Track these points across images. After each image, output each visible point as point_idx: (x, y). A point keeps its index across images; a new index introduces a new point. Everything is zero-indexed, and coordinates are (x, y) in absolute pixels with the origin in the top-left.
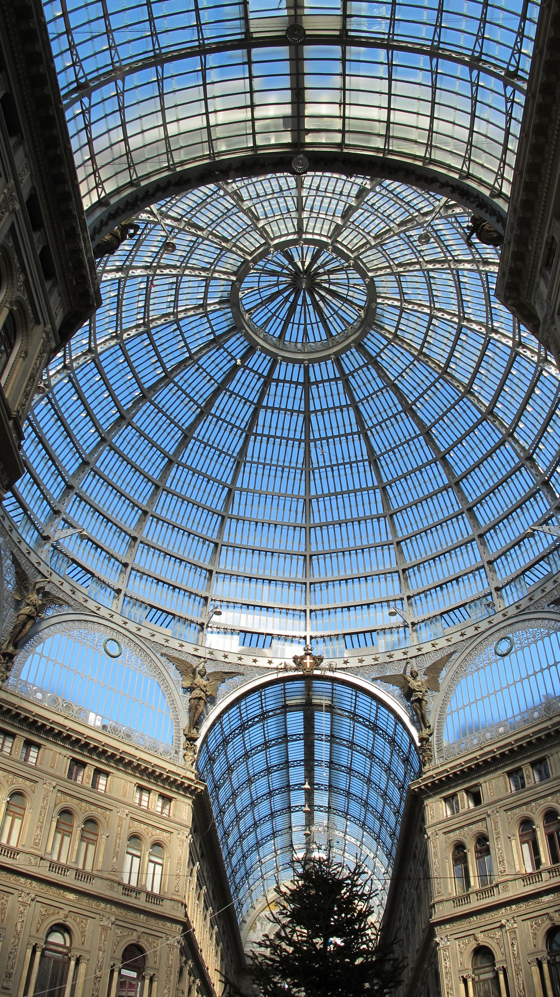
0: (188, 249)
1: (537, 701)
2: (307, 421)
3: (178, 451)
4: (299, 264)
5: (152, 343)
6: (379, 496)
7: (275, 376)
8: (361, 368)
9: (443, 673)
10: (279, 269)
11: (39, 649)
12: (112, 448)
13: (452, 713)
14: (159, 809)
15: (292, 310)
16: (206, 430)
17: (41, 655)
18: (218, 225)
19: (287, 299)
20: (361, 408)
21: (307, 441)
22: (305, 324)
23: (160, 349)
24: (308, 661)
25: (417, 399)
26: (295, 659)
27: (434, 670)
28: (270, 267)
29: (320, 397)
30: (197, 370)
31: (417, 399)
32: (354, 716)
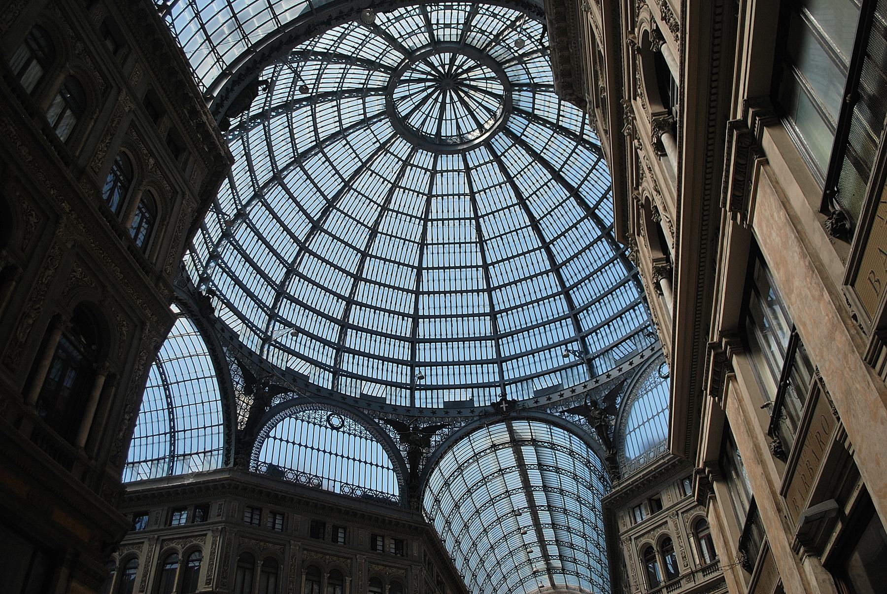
0: (340, 76)
2: (473, 201)
3: (368, 246)
4: (440, 68)
5: (328, 159)
6: (544, 253)
7: (439, 168)
8: (510, 148)
9: (619, 400)
10: (424, 76)
11: (272, 434)
12: (311, 253)
13: (630, 432)
14: (393, 551)
15: (443, 109)
16: (388, 224)
17: (275, 438)
18: (361, 50)
19: (436, 100)
20: (517, 182)
21: (477, 218)
22: (457, 119)
23: (335, 164)
24: (504, 405)
25: (563, 166)
26: (493, 404)
27: (611, 398)
28: (416, 76)
29: (480, 180)
30: (371, 175)
31: (563, 166)
32: (553, 446)
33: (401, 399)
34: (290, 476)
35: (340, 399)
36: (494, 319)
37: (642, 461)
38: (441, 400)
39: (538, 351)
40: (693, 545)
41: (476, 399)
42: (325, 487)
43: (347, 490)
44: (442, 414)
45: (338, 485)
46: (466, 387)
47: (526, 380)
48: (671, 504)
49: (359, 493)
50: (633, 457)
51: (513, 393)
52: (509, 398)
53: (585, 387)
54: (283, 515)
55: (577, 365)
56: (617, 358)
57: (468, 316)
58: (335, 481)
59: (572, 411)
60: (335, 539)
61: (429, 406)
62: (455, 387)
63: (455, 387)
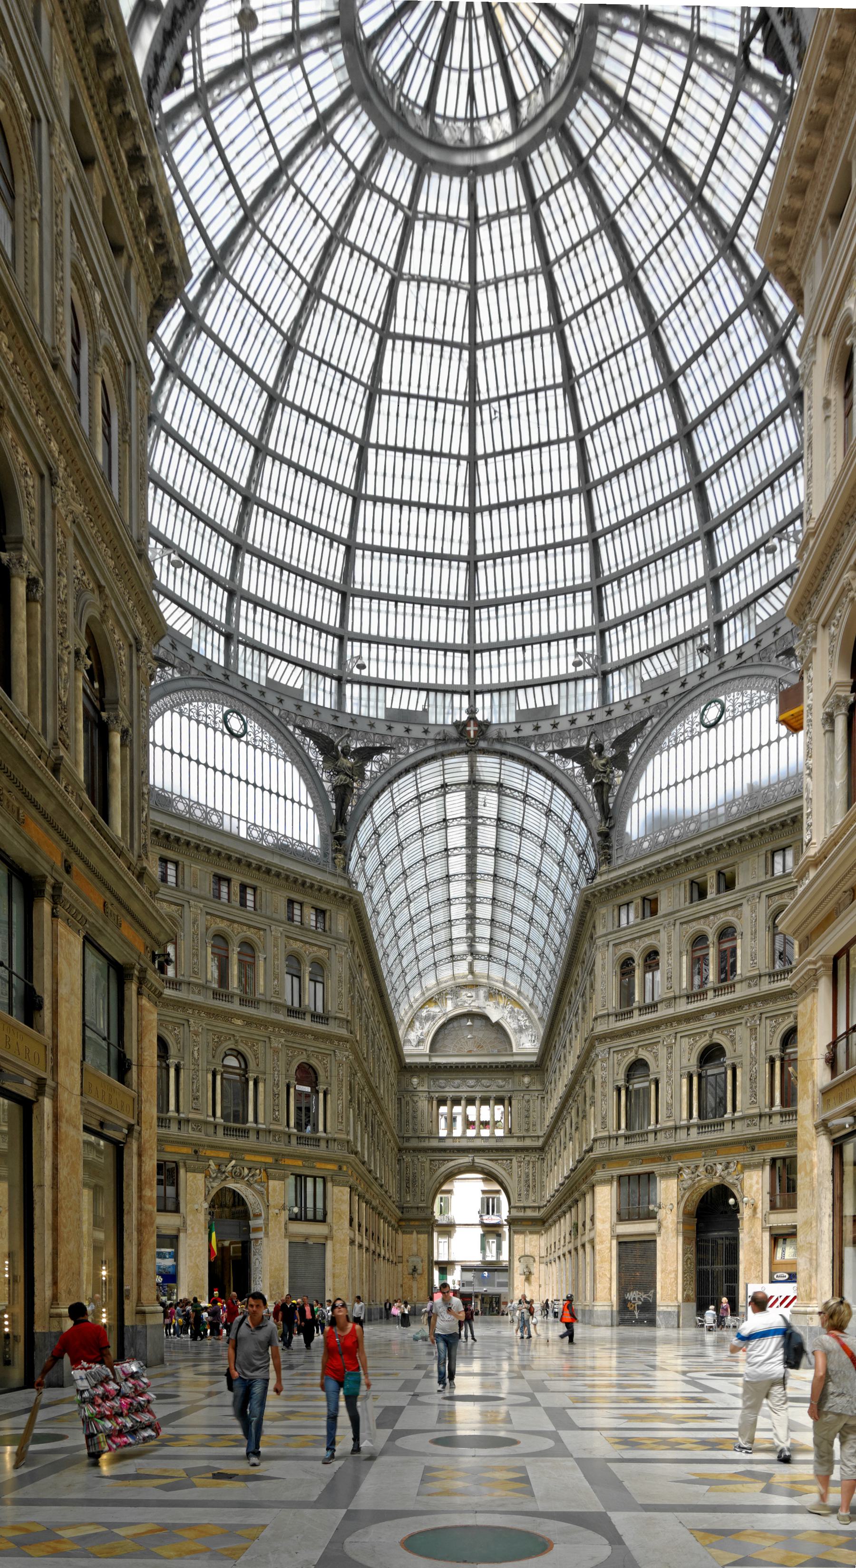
1: (738, 795)
13: (639, 801)
26: (457, 725)
33: (322, 694)
34: (181, 806)
35: (240, 687)
36: (472, 570)
37: (646, 845)
38: (381, 704)
39: (532, 641)
40: (684, 966)
41: (432, 710)
42: (226, 827)
43: (255, 834)
44: (382, 729)
45: (243, 825)
46: (419, 687)
47: (508, 689)
48: (670, 909)
49: (270, 839)
50: (634, 837)
51: (487, 709)
52: (479, 717)
53: (591, 717)
54: (176, 864)
55: (585, 678)
56: (646, 677)
57: (433, 556)
58: (239, 819)
59: (566, 753)
60: (243, 903)
61: (364, 712)
62: (403, 686)
63: (403, 686)
